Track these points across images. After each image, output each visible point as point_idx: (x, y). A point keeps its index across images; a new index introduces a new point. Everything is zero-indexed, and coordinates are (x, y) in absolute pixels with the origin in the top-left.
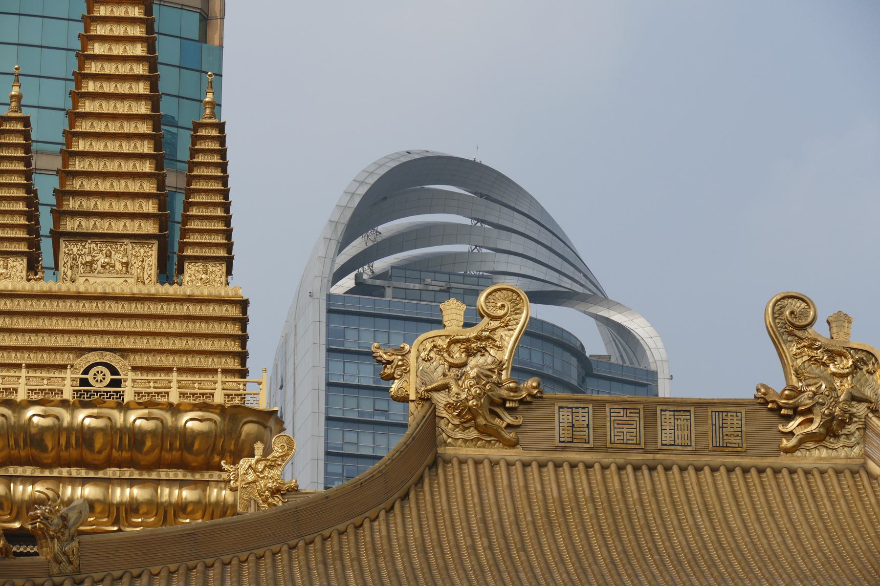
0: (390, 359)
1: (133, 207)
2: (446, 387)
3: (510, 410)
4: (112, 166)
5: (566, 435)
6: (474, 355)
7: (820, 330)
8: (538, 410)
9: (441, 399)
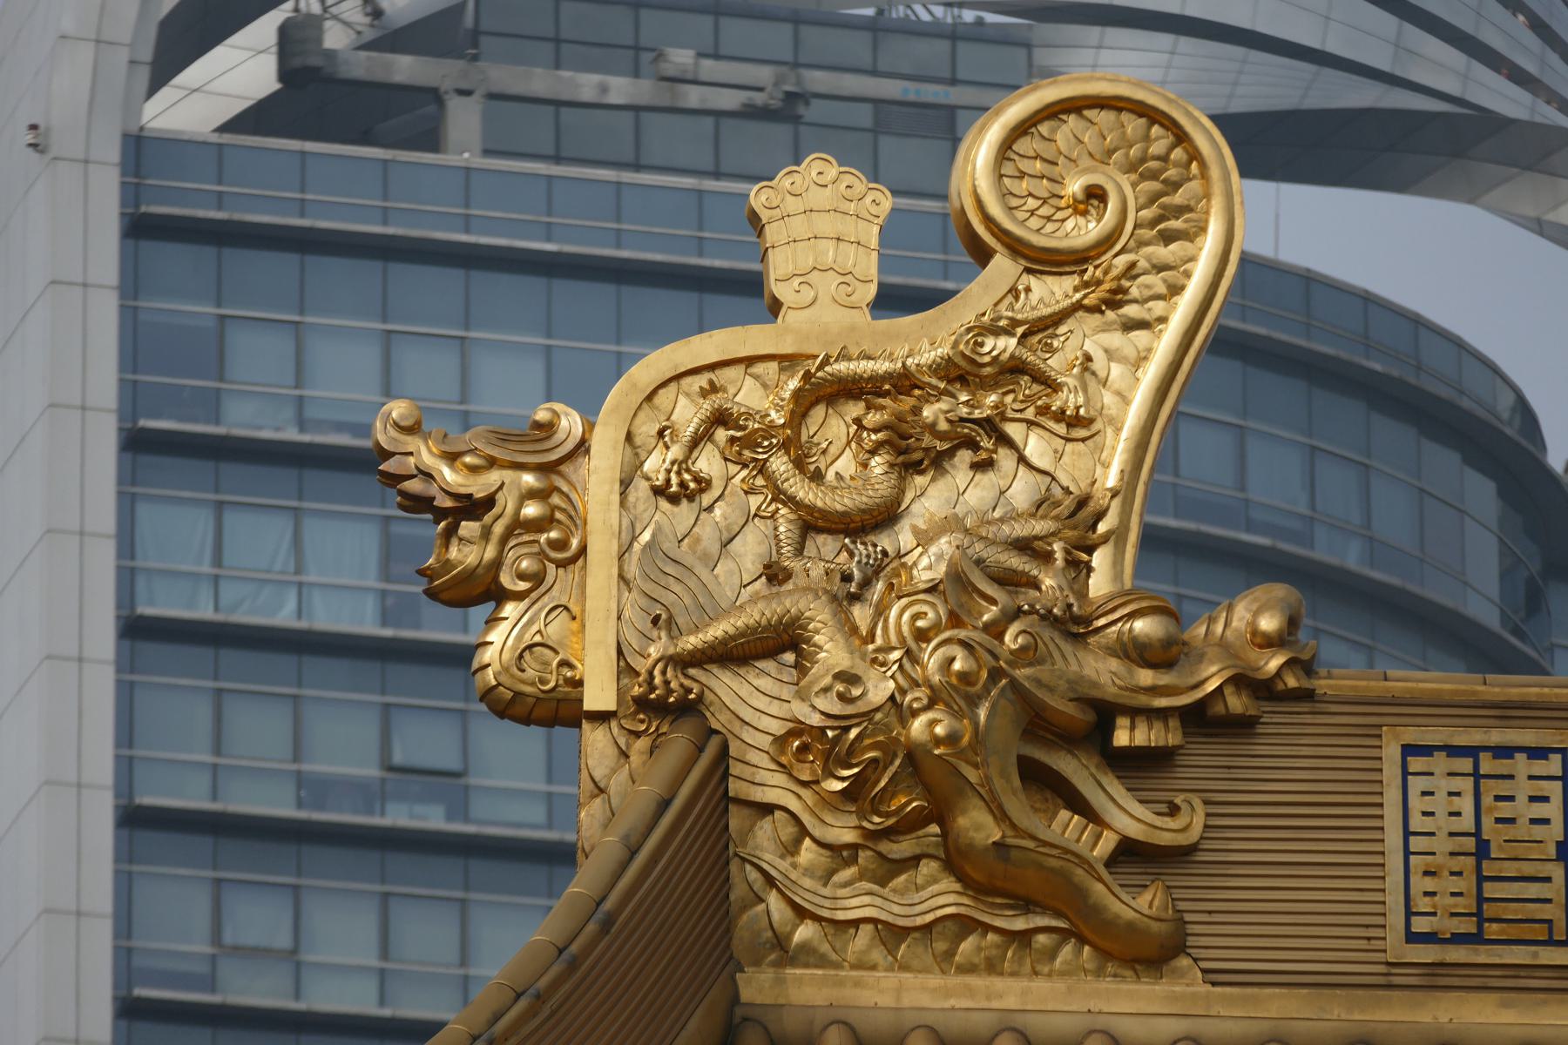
0: (478, 487)
2: (781, 642)
3: (1136, 766)
5: (1445, 899)
6: (938, 462)
8: (1286, 763)
9: (755, 703)
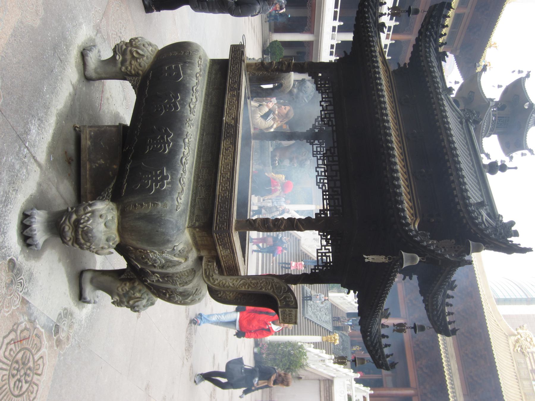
2: (521, 337)
9: (519, 336)
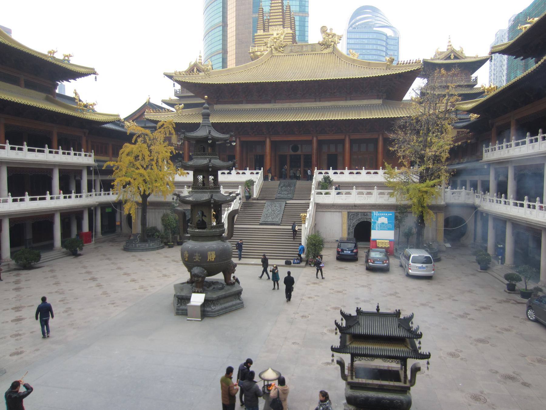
1: (279, 20)
4: (276, 14)
7: (328, 31)
8: (286, 47)
9: (273, 47)
